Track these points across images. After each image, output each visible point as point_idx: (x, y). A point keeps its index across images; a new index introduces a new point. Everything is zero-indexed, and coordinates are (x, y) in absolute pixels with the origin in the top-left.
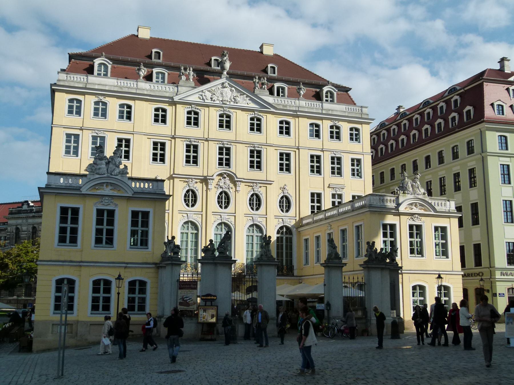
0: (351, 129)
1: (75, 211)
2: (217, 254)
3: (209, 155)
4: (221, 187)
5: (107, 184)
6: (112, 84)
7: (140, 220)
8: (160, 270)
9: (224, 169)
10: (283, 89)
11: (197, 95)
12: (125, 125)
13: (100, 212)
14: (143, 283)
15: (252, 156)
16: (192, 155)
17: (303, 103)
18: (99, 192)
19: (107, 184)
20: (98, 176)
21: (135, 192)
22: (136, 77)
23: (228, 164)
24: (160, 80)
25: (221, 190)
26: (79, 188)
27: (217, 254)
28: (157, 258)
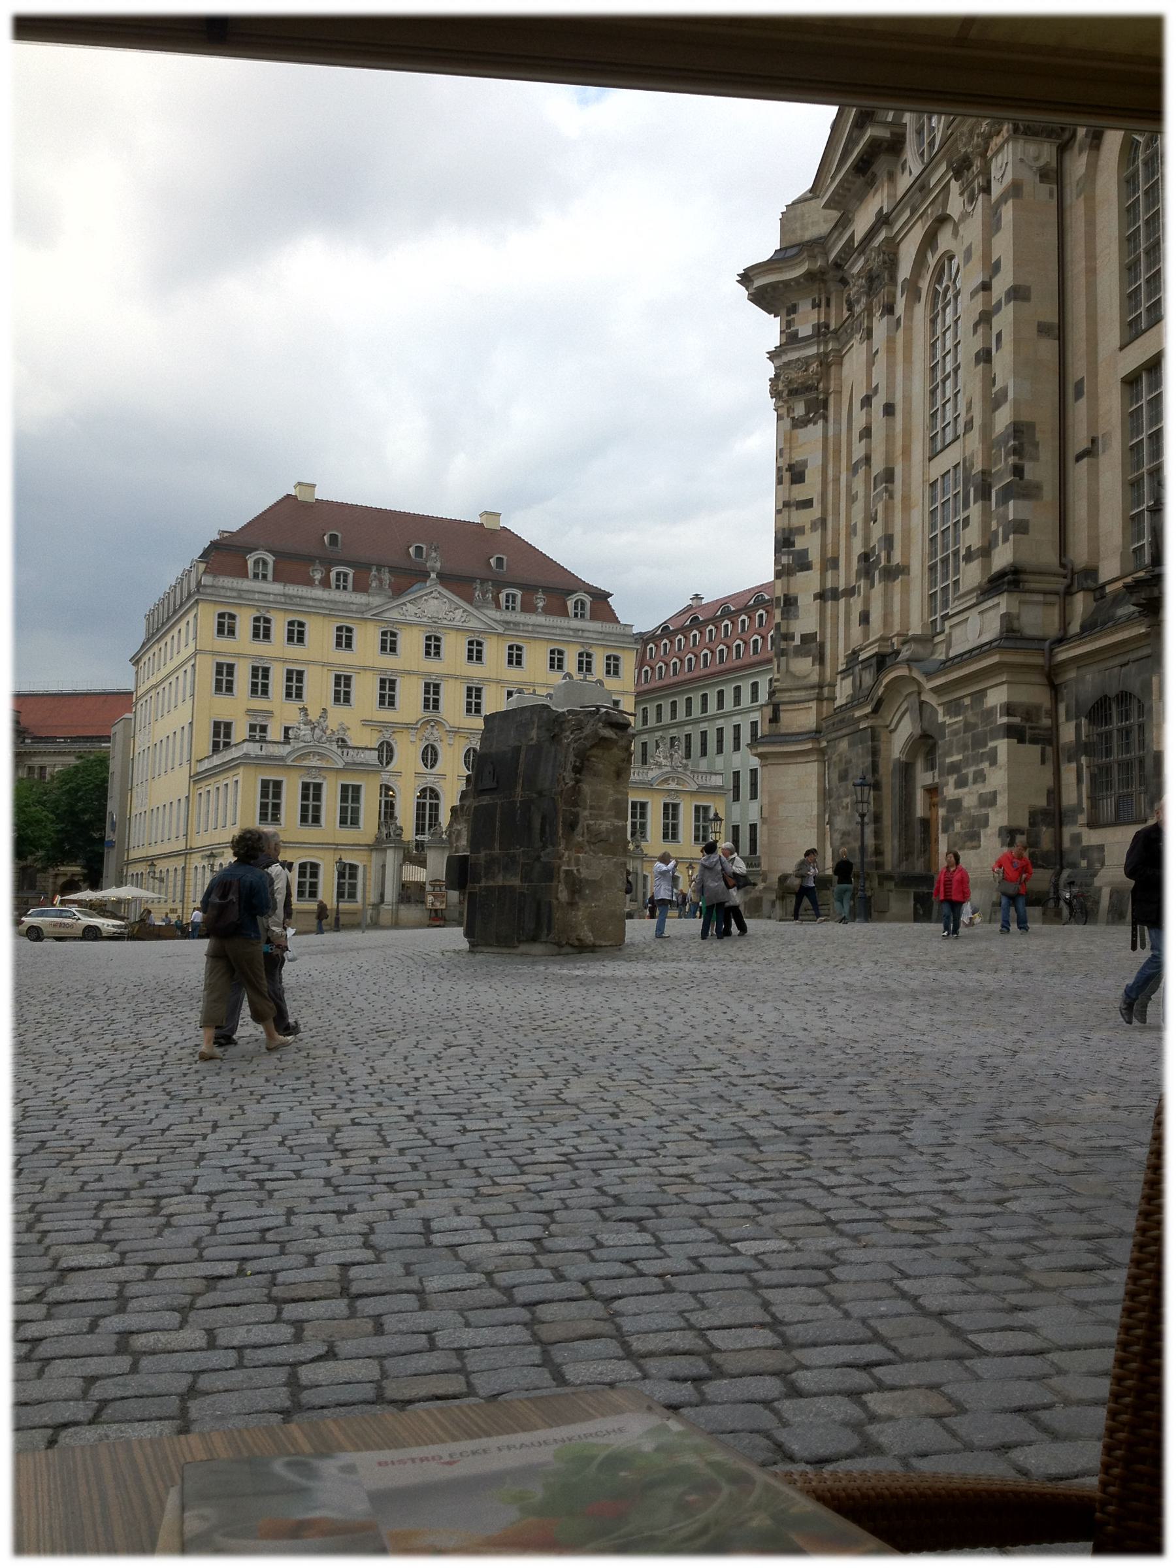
1: (278, 784)
2: (444, 836)
3: (410, 695)
5: (315, 753)
6: (276, 592)
7: (350, 794)
8: (374, 854)
9: (430, 715)
10: (514, 596)
12: (295, 651)
13: (306, 786)
14: (353, 867)
15: (469, 696)
16: (387, 693)
17: (541, 619)
18: (305, 763)
19: (315, 753)
20: (303, 744)
21: (347, 763)
22: (309, 582)
23: (436, 707)
24: (342, 584)
26: (282, 758)
27: (444, 836)
28: (370, 840)
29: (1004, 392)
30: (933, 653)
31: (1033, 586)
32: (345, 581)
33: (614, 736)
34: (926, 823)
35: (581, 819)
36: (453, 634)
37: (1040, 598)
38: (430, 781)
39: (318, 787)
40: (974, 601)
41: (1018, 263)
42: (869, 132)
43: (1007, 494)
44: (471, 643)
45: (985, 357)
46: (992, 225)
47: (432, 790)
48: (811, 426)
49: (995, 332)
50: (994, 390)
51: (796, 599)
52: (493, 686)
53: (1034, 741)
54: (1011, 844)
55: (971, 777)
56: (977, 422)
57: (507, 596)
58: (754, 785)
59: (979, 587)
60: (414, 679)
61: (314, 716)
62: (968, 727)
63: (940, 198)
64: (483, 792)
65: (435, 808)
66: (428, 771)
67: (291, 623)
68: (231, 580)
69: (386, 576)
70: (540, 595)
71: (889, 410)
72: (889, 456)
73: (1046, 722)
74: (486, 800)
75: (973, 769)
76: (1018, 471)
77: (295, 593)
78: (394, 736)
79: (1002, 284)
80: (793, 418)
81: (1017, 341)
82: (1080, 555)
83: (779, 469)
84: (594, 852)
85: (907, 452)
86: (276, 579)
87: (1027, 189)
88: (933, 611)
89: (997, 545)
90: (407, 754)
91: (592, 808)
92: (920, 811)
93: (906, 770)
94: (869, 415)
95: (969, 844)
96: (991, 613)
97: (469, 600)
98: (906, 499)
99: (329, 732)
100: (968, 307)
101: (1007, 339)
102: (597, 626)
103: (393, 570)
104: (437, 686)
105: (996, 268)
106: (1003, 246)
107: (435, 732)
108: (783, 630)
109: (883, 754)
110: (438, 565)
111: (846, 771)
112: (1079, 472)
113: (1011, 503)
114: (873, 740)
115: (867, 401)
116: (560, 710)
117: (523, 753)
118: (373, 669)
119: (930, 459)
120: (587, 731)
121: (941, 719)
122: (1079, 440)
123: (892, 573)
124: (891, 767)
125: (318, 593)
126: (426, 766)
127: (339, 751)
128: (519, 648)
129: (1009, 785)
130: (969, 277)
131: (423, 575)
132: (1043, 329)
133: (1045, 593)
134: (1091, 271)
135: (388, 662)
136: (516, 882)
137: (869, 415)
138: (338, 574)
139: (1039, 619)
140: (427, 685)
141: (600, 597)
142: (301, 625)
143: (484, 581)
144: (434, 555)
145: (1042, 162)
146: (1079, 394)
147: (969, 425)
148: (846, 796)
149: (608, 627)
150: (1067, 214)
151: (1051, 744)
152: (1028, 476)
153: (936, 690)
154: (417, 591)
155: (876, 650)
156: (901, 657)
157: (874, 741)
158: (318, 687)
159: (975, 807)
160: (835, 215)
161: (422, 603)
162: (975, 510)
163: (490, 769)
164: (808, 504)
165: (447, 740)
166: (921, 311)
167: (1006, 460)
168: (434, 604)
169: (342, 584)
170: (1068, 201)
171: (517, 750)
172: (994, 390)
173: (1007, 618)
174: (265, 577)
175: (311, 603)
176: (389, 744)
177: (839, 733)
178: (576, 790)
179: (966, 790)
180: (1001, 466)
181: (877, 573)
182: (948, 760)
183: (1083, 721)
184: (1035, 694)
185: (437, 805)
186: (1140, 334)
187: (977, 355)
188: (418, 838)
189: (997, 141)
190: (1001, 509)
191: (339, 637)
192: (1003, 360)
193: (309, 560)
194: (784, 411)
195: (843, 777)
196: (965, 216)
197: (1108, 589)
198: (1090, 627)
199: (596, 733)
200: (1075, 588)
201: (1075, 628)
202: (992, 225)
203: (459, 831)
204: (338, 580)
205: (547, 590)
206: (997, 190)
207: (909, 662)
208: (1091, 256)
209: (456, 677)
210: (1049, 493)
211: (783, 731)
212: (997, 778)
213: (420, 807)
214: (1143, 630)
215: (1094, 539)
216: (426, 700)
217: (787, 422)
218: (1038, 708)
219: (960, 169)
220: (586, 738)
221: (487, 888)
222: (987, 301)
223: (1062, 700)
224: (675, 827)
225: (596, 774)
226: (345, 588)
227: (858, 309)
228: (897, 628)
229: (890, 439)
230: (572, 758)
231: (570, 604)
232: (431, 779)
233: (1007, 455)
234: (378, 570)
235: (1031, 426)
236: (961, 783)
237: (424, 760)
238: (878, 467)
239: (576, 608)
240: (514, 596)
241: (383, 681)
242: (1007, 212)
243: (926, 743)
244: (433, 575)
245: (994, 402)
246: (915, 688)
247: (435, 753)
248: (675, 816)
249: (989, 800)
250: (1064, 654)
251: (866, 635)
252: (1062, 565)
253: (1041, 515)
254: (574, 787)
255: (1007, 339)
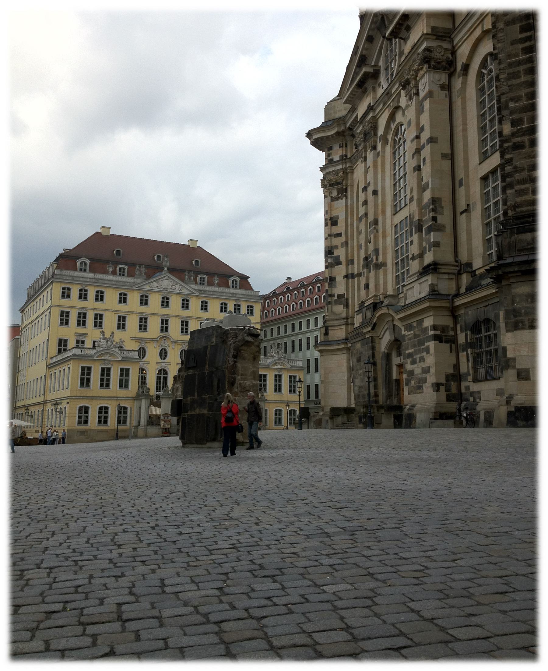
0: (248, 306)
2: (170, 392)
3: (154, 325)
4: (162, 346)
7: (125, 373)
9: (163, 334)
10: (204, 278)
11: (148, 285)
12: (99, 305)
15: (182, 325)
16: (143, 324)
17: (217, 289)
22: (107, 273)
23: (166, 331)
24: (122, 273)
25: (162, 347)
27: (170, 392)
29: (427, 184)
30: (398, 302)
31: (443, 271)
32: (123, 272)
33: (252, 341)
34: (398, 381)
35: (237, 380)
36: (175, 296)
37: (446, 276)
38: (163, 366)
39: (109, 369)
40: (417, 278)
41: (431, 127)
42: (364, 70)
43: (430, 229)
44: (183, 300)
45: (418, 168)
46: (420, 110)
47: (164, 370)
48: (340, 200)
49: (422, 157)
50: (423, 183)
51: (335, 278)
52: (194, 320)
53: (446, 342)
54: (438, 390)
55: (418, 360)
56: (415, 198)
57: (201, 278)
58: (317, 365)
59: (419, 272)
60: (156, 317)
61: (107, 335)
62: (416, 336)
63: (396, 98)
64: (189, 368)
65: (166, 379)
66: (163, 361)
67: (97, 292)
68: (69, 272)
69: (143, 269)
70: (216, 278)
71: (375, 193)
72: (376, 213)
73: (452, 333)
74: (191, 372)
75: (419, 356)
76: (434, 219)
77: (99, 277)
78: (146, 344)
79: (425, 136)
80: (332, 197)
81: (432, 161)
82: (464, 257)
83: (326, 220)
84: (243, 396)
85: (384, 212)
86: (90, 271)
87: (435, 94)
88: (398, 283)
89: (426, 253)
90: (153, 353)
91: (242, 375)
92: (395, 376)
93: (388, 357)
94: (366, 195)
95: (418, 391)
96: (426, 283)
97: (183, 280)
98: (384, 232)
99: (114, 343)
100: (410, 147)
101: (428, 161)
102: (242, 292)
103: (146, 266)
104: (167, 321)
105: (422, 129)
106: (425, 119)
107: (166, 342)
108: (329, 293)
109: (377, 349)
110: (168, 264)
111: (360, 357)
112: (462, 219)
113: (432, 233)
114: (372, 342)
115: (365, 189)
116: (227, 328)
117: (209, 349)
118: (136, 313)
119: (394, 215)
120: (240, 338)
121: (403, 333)
122: (462, 205)
123: (378, 266)
124: (381, 355)
125: (111, 277)
126: (161, 359)
127: (119, 352)
128: (206, 302)
129: (436, 363)
130: (410, 134)
131: (161, 269)
132: (444, 156)
133: (449, 274)
134: (465, 130)
135: (144, 309)
136: (205, 412)
137: (366, 195)
138: (120, 269)
139: (446, 286)
140: (162, 320)
141: (244, 278)
142: (102, 292)
143: (189, 271)
144: (166, 259)
145: (441, 82)
146: (461, 184)
147: (412, 199)
148: (360, 369)
149: (248, 292)
150: (454, 105)
151: (454, 343)
152: (439, 221)
153: (400, 319)
154: (158, 276)
155: (372, 301)
156: (384, 304)
157: (373, 343)
158: (110, 322)
159: (420, 374)
160: (349, 106)
161: (160, 282)
162: (415, 237)
163: (192, 358)
164: (339, 235)
165: (171, 346)
166: (388, 149)
167: (429, 214)
168: (166, 282)
169: (122, 273)
170: (453, 100)
171: (206, 348)
172: (423, 183)
173: (432, 286)
174: (85, 270)
175: (107, 282)
176: (144, 349)
177: (356, 340)
178: (234, 366)
179: (416, 366)
180: (427, 217)
181: (372, 266)
182: (407, 352)
183: (468, 332)
184: (446, 321)
185: (166, 377)
186: (487, 158)
187: (414, 168)
188: (157, 393)
189: (421, 73)
190: (427, 237)
191: (120, 298)
192: (426, 170)
193: (107, 262)
194: (327, 194)
195: (359, 360)
196: (408, 106)
197: (477, 273)
198: (470, 289)
199: (244, 339)
200: (462, 271)
201: (463, 290)
202: (420, 110)
203: (178, 388)
204: (120, 271)
205: (219, 275)
206: (422, 94)
207: (388, 306)
208: (465, 124)
209: (177, 316)
210: (449, 229)
211: (330, 339)
212: (430, 360)
213: (158, 378)
214: (494, 291)
215: (470, 250)
216: (162, 327)
217: (329, 198)
218: (448, 327)
219: (405, 85)
220: (238, 341)
221: (191, 415)
222: (418, 143)
223: (459, 323)
224: (280, 386)
225: (244, 359)
226: (123, 275)
227: (360, 148)
228: (381, 291)
229: (376, 206)
230: (232, 351)
231: (230, 282)
232: (163, 365)
233: (429, 212)
234: (140, 267)
235: (440, 199)
236: (414, 362)
237: (161, 356)
238: (371, 218)
239: (233, 283)
240: (204, 278)
241: (141, 319)
242: (427, 105)
243: (397, 344)
244: (166, 269)
245: (423, 189)
246: (391, 319)
247: (166, 352)
248: (280, 381)
249: (426, 370)
250: (458, 302)
251: (368, 295)
252: (456, 261)
253: (446, 239)
254: (233, 365)
255: (428, 161)
